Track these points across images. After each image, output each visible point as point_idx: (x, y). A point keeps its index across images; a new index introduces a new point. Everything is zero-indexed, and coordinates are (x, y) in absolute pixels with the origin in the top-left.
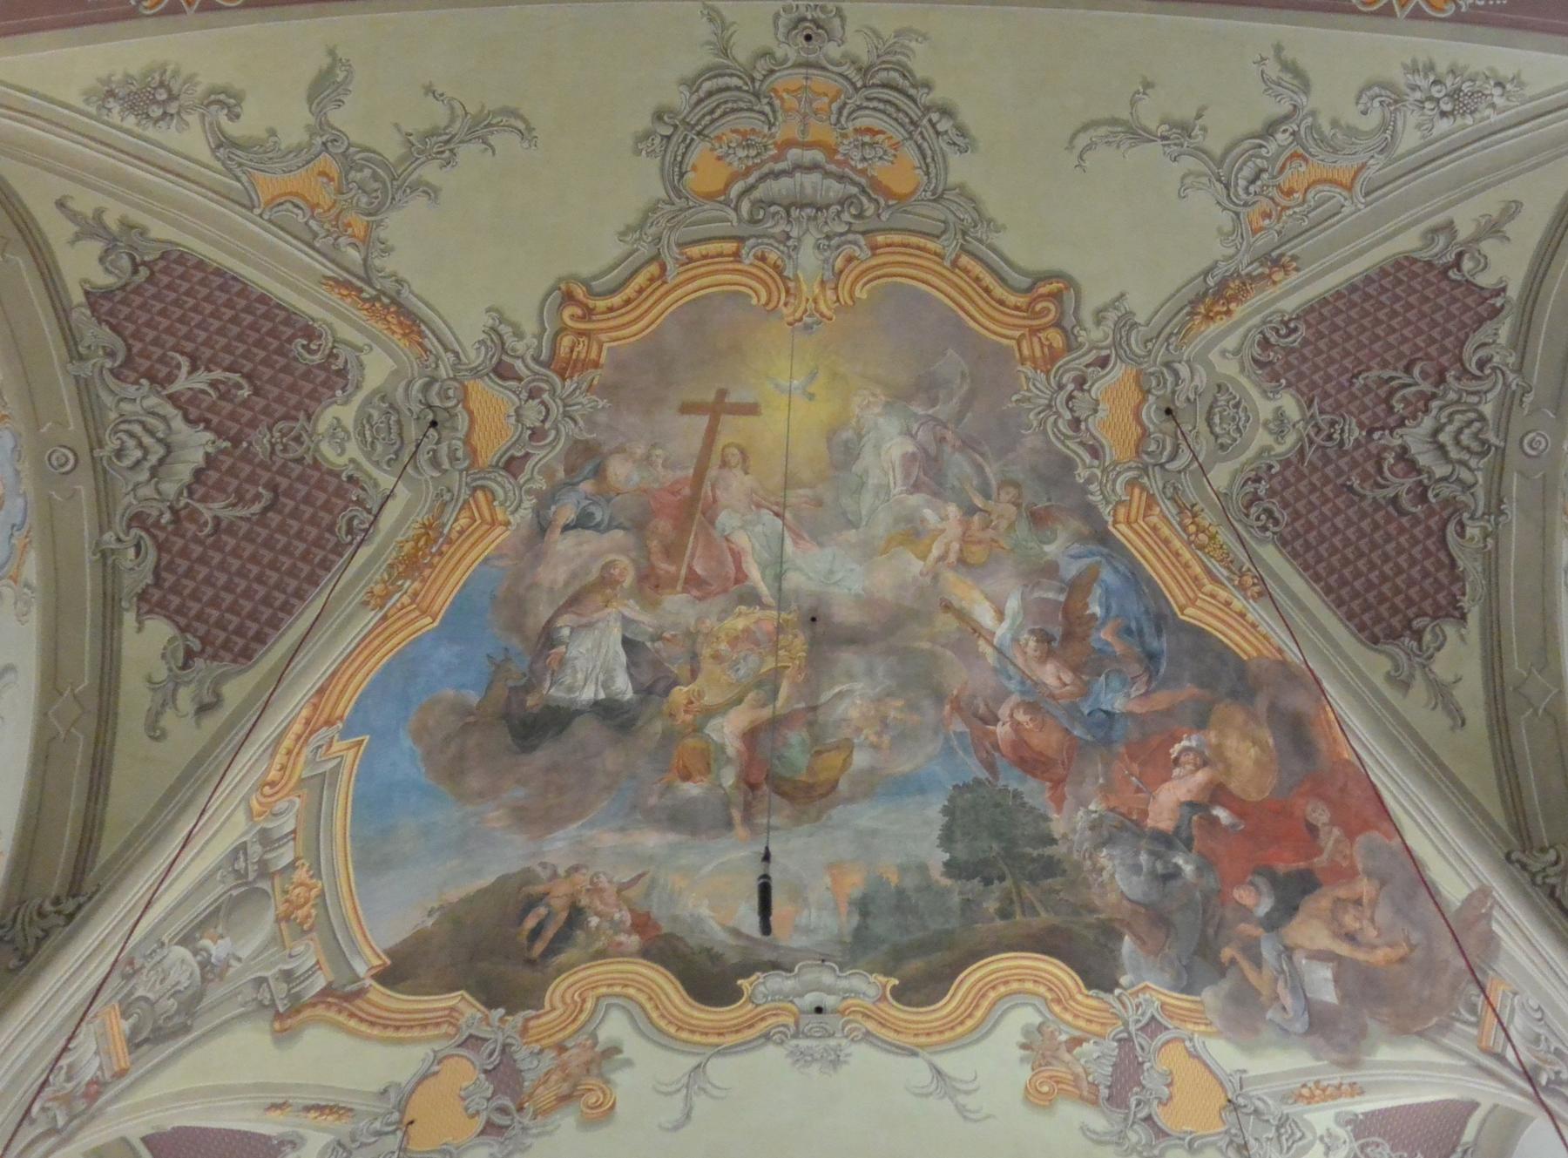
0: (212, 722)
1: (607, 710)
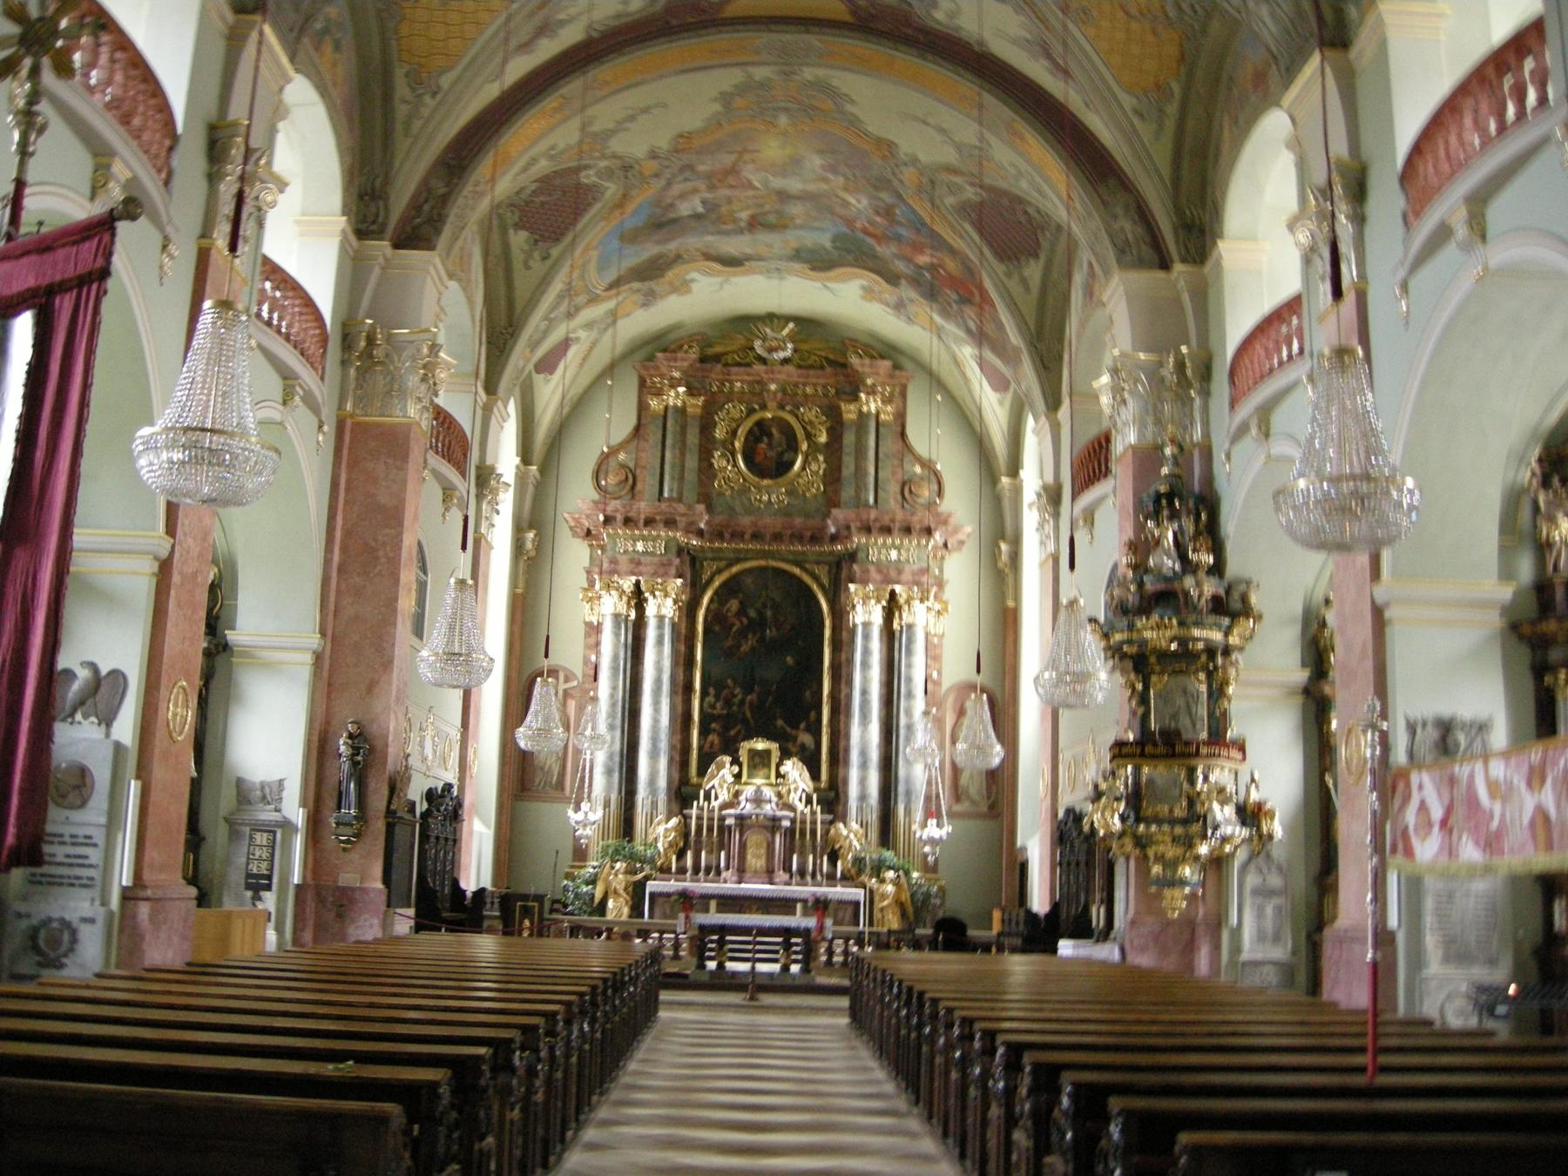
0: (549, 263)
1: (697, 217)
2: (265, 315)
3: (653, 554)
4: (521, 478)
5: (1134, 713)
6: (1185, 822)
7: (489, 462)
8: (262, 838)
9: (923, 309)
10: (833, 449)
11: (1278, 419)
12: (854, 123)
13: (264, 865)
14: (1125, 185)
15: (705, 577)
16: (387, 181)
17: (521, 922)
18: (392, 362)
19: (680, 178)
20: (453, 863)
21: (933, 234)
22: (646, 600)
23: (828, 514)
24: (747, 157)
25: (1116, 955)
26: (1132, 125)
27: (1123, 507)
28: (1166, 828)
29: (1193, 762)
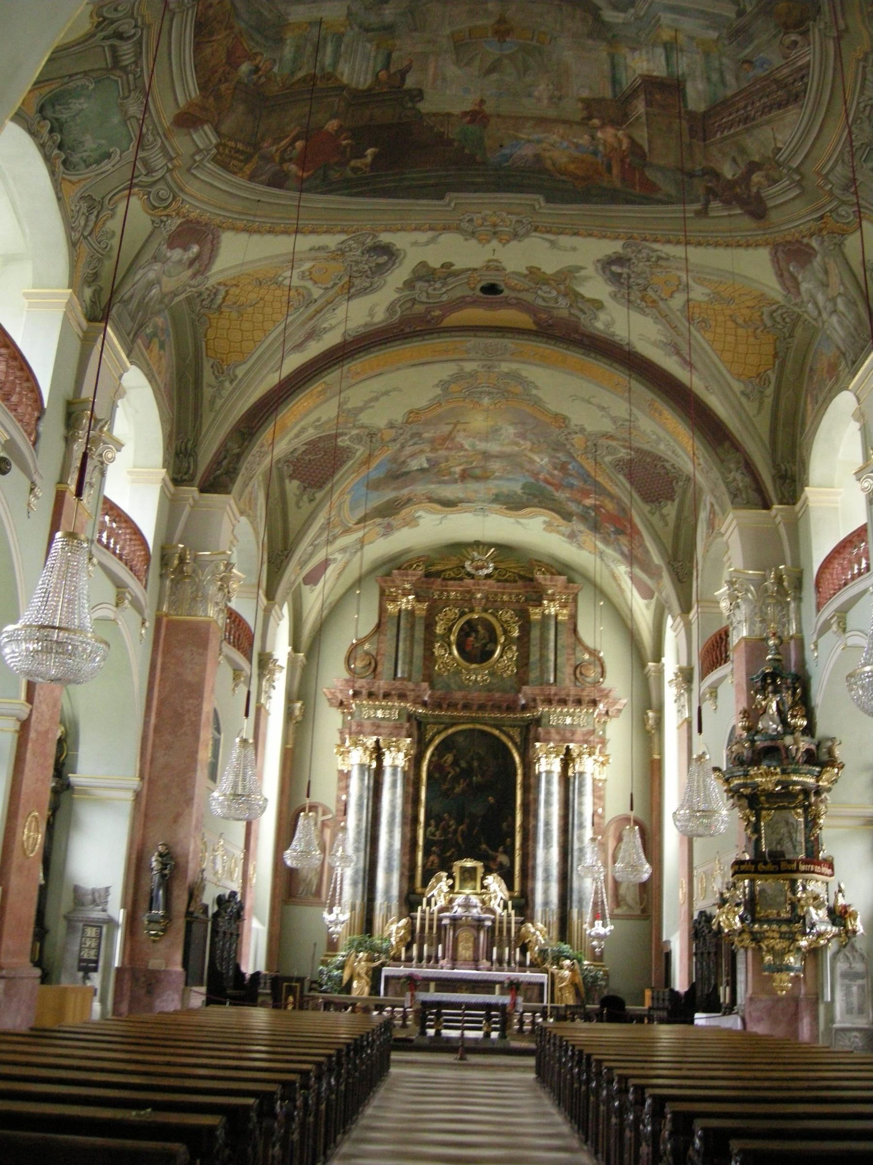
0: (314, 504)
1: (422, 470)
2: (104, 540)
3: (389, 719)
4: (292, 662)
5: (749, 839)
6: (788, 922)
7: (268, 651)
8: (91, 932)
9: (588, 537)
10: (523, 642)
11: (853, 618)
12: (537, 403)
13: (93, 952)
14: (736, 446)
15: (428, 737)
16: (196, 445)
17: (286, 999)
18: (197, 576)
19: (411, 443)
20: (236, 952)
21: (596, 483)
22: (383, 754)
23: (519, 691)
24: (459, 427)
25: (739, 1025)
26: (741, 404)
27: (737, 685)
28: (775, 927)
29: (795, 876)
